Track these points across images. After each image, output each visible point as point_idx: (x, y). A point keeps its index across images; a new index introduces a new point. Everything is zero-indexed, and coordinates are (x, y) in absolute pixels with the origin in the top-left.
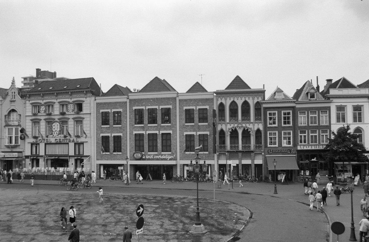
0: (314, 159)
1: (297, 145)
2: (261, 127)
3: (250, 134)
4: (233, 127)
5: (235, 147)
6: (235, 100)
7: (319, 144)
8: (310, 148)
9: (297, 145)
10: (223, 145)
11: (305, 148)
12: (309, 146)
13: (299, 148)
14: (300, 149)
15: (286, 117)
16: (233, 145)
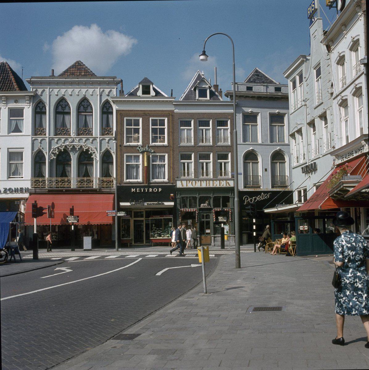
0: (204, 203)
1: (176, 179)
2: (113, 147)
3: (92, 159)
4: (61, 146)
5: (63, 181)
6: (65, 97)
7: (215, 179)
8: (198, 185)
9: (176, 179)
10: (41, 179)
11: (190, 185)
12: (197, 182)
13: (179, 185)
14: (181, 187)
15: (157, 128)
16: (60, 179)
